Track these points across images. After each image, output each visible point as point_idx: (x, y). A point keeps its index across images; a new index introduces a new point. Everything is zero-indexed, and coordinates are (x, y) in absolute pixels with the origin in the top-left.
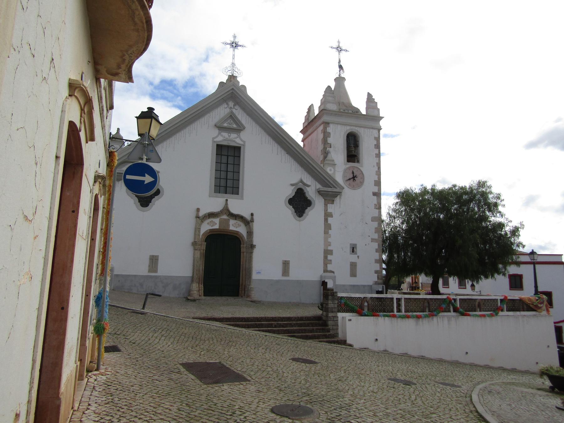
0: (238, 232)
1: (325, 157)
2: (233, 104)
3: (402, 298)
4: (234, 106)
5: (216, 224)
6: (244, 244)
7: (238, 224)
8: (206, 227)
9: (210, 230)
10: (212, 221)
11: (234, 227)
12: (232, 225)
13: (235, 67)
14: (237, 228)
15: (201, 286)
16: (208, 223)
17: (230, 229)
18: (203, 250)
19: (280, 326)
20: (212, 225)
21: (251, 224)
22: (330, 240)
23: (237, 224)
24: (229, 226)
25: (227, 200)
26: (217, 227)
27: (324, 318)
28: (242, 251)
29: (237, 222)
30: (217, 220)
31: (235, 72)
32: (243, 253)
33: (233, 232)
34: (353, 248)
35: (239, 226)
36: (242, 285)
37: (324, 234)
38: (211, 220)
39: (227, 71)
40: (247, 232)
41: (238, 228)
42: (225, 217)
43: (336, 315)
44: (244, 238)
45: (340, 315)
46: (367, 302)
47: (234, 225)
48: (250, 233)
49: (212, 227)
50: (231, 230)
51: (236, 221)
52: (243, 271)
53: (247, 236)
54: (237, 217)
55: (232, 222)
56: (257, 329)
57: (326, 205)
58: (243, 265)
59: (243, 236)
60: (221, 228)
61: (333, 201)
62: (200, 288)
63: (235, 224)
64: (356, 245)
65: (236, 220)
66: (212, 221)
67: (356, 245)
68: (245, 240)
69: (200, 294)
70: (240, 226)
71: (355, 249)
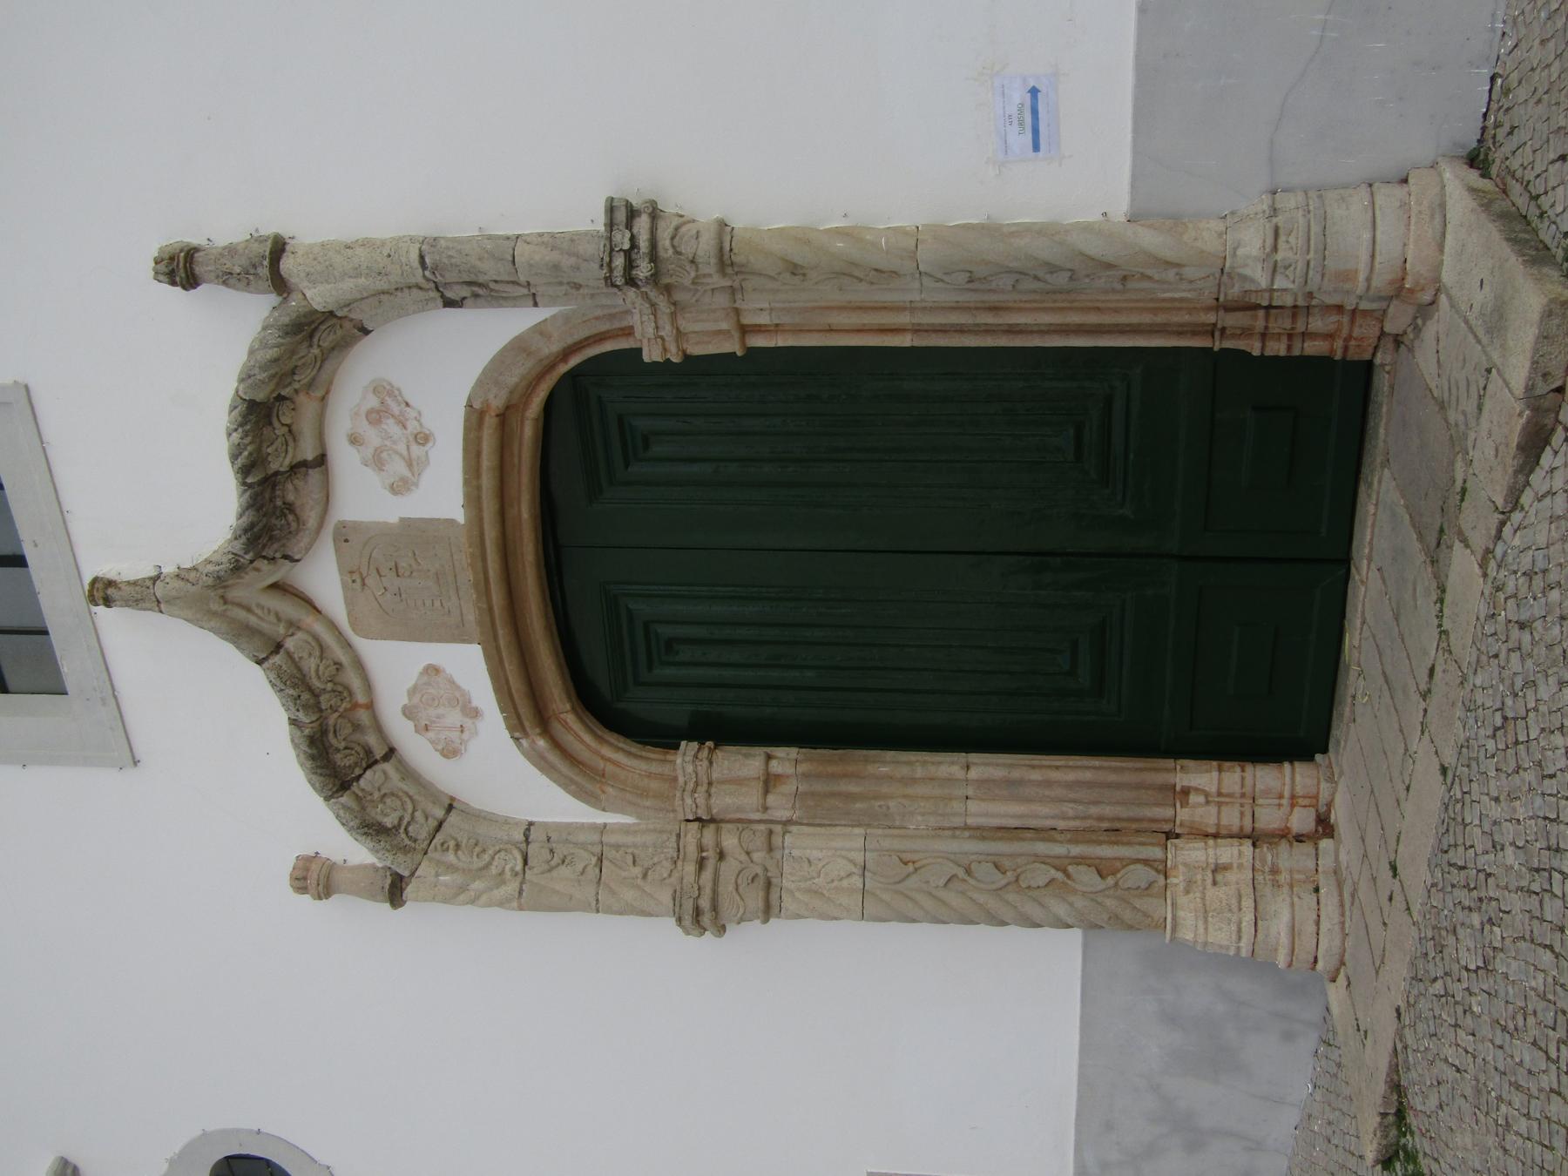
0: (475, 417)
5: (432, 670)
6: (628, 332)
7: (376, 417)
9: (517, 727)
10: (408, 712)
12: (399, 488)
14: (423, 438)
15: (1196, 812)
17: (459, 515)
18: (769, 782)
20: (454, 717)
21: (318, 296)
23: (372, 436)
24: (417, 533)
25: (103, 592)
28: (732, 346)
29: (354, 440)
32: (745, 330)
33: (488, 482)
36: (1211, 330)
41: (430, 423)
44: (540, 330)
47: (398, 467)
49: (475, 713)
50: (473, 499)
51: (346, 462)
52: (1012, 330)
54: (279, 464)
58: (917, 330)
59: (519, 346)
60: (471, 616)
62: (1232, 818)
63: (377, 461)
65: (321, 460)
66: (408, 712)
69: (1302, 820)
70: (384, 390)
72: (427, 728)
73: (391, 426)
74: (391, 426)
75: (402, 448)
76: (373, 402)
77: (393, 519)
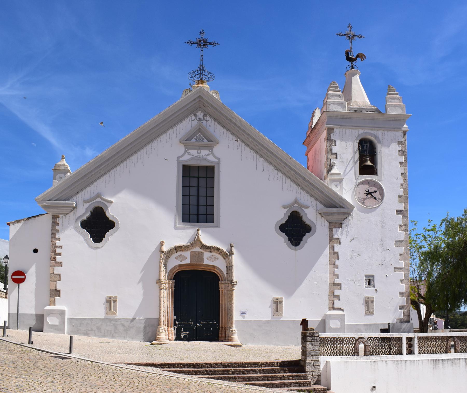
1: (329, 171)
2: (202, 114)
3: (415, 337)
4: (204, 117)
5: (186, 258)
7: (215, 258)
8: (174, 262)
9: (180, 266)
10: (181, 255)
11: (210, 260)
13: (204, 69)
16: (176, 258)
19: (239, 372)
20: (180, 259)
22: (337, 272)
24: (202, 259)
26: (187, 261)
27: (302, 363)
30: (187, 254)
31: (204, 76)
34: (369, 280)
35: (216, 259)
37: (329, 264)
38: (179, 253)
39: (193, 76)
40: (227, 267)
42: (197, 249)
43: (317, 359)
45: (323, 360)
46: (364, 343)
47: (210, 259)
48: (229, 268)
53: (227, 271)
55: (206, 255)
56: (206, 376)
57: (331, 230)
59: (221, 271)
61: (341, 224)
64: (373, 276)
65: (211, 252)
67: (373, 276)
68: (224, 276)
70: (218, 259)
71: (372, 281)
72: (179, 257)
73: (214, 259)
74: (214, 259)
75: (211, 260)
76: (216, 258)
77: (204, 257)
